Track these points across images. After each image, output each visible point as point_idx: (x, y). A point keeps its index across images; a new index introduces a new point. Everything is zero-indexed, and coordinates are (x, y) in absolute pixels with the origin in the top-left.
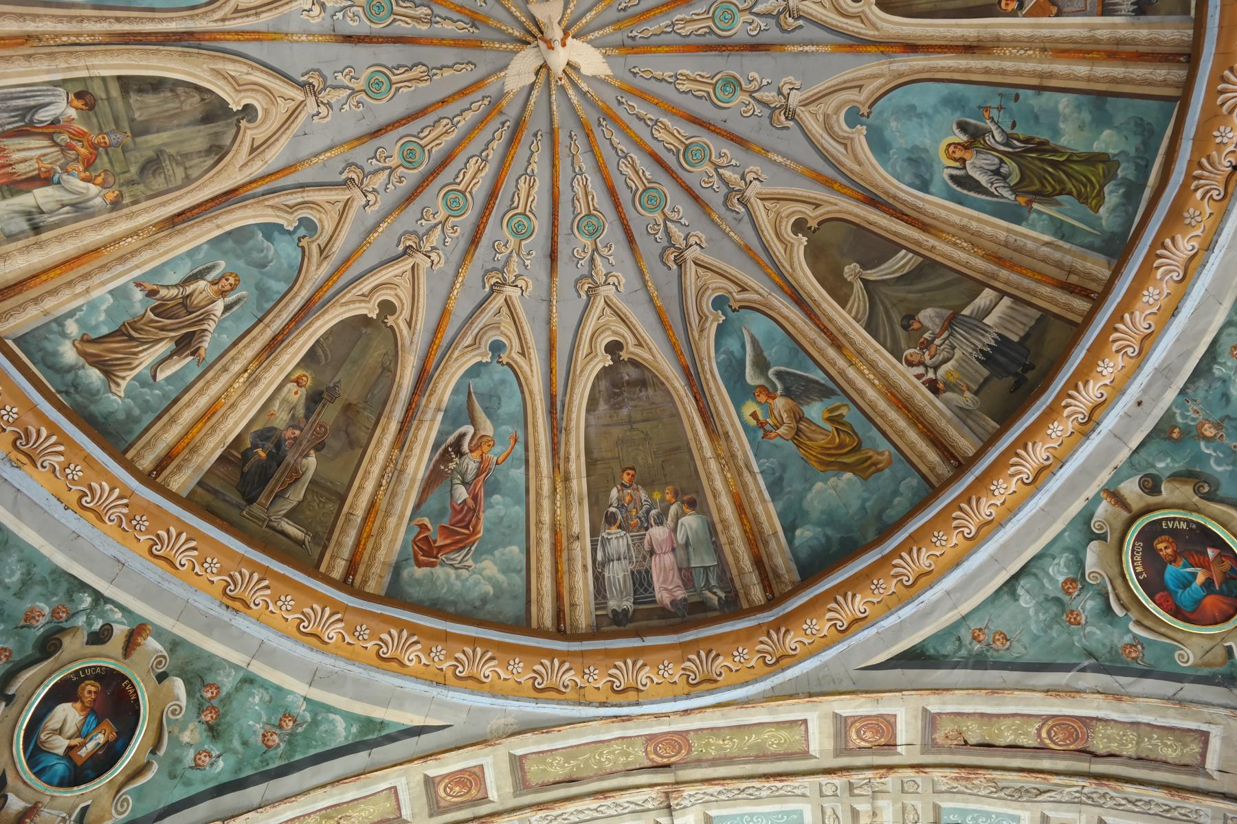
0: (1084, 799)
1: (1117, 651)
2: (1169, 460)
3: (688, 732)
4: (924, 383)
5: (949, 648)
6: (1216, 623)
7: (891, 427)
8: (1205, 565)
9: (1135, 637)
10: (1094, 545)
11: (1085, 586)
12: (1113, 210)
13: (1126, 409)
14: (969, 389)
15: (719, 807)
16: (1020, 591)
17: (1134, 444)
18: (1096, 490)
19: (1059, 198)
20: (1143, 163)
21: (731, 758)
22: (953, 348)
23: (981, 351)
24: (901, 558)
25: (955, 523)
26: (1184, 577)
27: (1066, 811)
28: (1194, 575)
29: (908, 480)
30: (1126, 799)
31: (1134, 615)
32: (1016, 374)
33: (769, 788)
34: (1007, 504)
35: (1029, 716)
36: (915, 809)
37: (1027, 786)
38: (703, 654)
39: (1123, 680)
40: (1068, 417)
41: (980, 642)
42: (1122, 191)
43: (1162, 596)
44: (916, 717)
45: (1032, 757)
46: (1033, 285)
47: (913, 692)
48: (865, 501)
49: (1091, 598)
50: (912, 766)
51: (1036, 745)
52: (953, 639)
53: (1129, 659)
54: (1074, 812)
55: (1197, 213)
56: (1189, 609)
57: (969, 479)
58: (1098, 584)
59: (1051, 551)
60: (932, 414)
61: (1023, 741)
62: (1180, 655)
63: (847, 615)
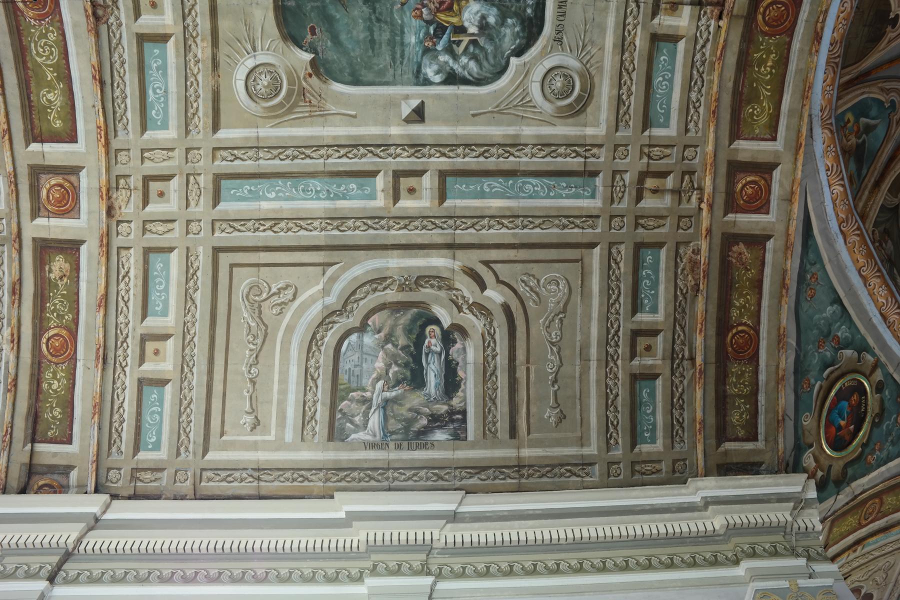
0: (677, 361)
3: (791, 36)
5: (811, 256)
8: (847, 425)
9: (814, 386)
10: (856, 354)
11: (836, 350)
15: (686, 51)
16: (835, 306)
21: (745, 70)
28: (843, 420)
31: (825, 384)
33: (698, 100)
44: (764, 229)
49: (831, 354)
54: (664, 354)
63: (833, 180)
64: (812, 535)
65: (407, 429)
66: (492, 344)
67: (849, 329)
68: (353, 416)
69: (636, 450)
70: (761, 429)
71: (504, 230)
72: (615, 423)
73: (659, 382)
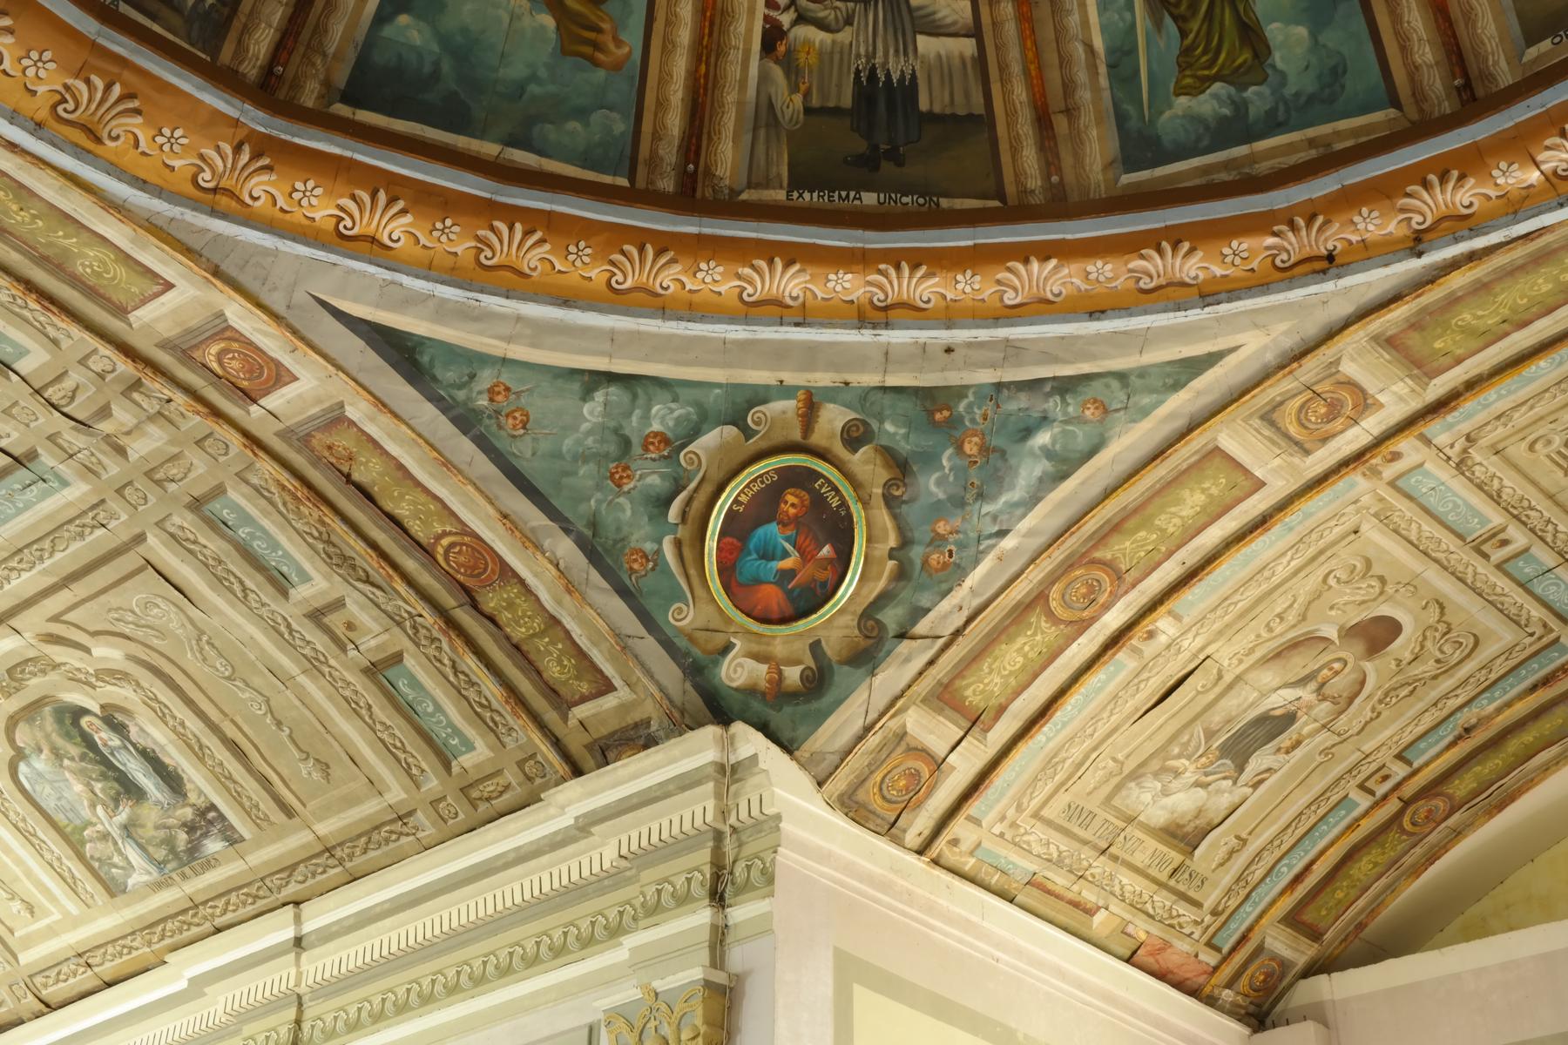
1: (624, 547)
2: (902, 431)
4: (766, 18)
5: (448, 375)
6: (748, 615)
7: (668, 23)
9: (659, 552)
10: (731, 431)
11: (672, 458)
12: (1194, 118)
13: (929, 341)
14: (807, 95)
16: (599, 396)
17: (893, 380)
18: (802, 383)
19: (1168, 21)
20: (1281, 116)
22: (849, 21)
23: (873, 69)
24: (511, 228)
25: (617, 257)
26: (775, 548)
27: (371, 617)
28: (786, 555)
29: (615, 115)
30: (454, 662)
31: (682, 532)
32: (876, 147)
34: (696, 298)
35: (453, 514)
36: (189, 470)
37: (359, 562)
38: (117, 90)
39: (595, 576)
40: (869, 283)
41: (491, 400)
42: (1226, 111)
43: (732, 544)
45: (403, 548)
46: (1016, 68)
47: (353, 384)
48: (533, 78)
49: (663, 476)
50: (246, 434)
51: (424, 541)
52: (467, 371)
53: (626, 566)
54: (380, 624)
55: (1245, 255)
56: (741, 579)
57: (689, 226)
58: (686, 470)
59: (679, 390)
60: (733, 70)
61: (415, 528)
62: (680, 609)
63: (369, 224)
64: (766, 827)
65: (172, 850)
66: (166, 711)
67: (675, 400)
68: (110, 858)
69: (455, 769)
70: (609, 670)
71: (25, 575)
72: (399, 745)
73: (409, 662)
